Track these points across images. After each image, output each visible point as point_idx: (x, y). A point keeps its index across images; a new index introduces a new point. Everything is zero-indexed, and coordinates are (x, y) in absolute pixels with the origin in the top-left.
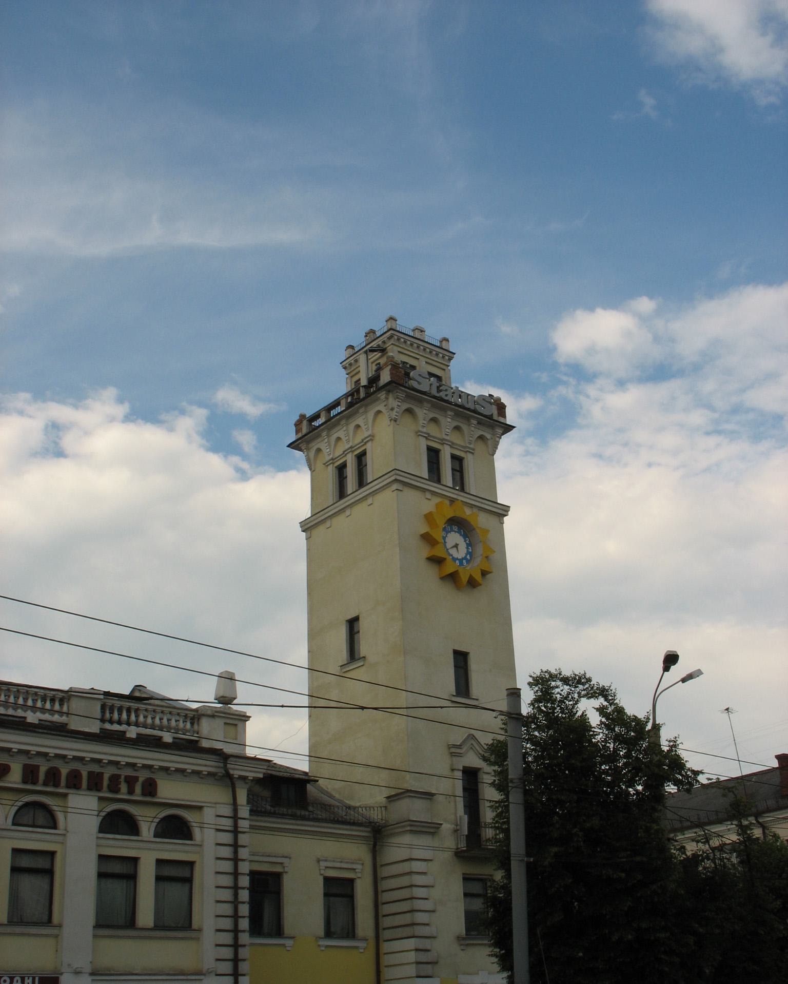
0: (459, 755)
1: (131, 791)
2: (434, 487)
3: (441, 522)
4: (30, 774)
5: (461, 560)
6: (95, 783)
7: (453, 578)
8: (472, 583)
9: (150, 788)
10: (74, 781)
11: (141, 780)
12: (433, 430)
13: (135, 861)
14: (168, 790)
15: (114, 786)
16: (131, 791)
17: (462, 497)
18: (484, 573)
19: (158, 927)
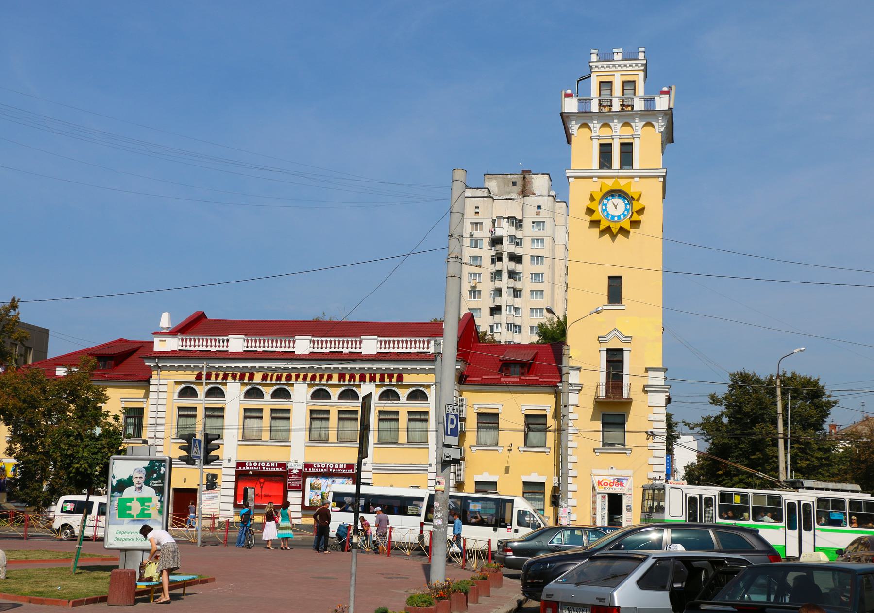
0: (606, 341)
1: (391, 381)
2: (605, 172)
3: (598, 197)
4: (342, 376)
5: (619, 217)
6: (373, 379)
7: (608, 230)
8: (623, 231)
9: (400, 378)
10: (362, 379)
11: (395, 375)
12: (606, 132)
13: (397, 413)
14: (408, 379)
15: (382, 379)
16: (391, 381)
17: (626, 172)
18: (636, 224)
19: (409, 442)
